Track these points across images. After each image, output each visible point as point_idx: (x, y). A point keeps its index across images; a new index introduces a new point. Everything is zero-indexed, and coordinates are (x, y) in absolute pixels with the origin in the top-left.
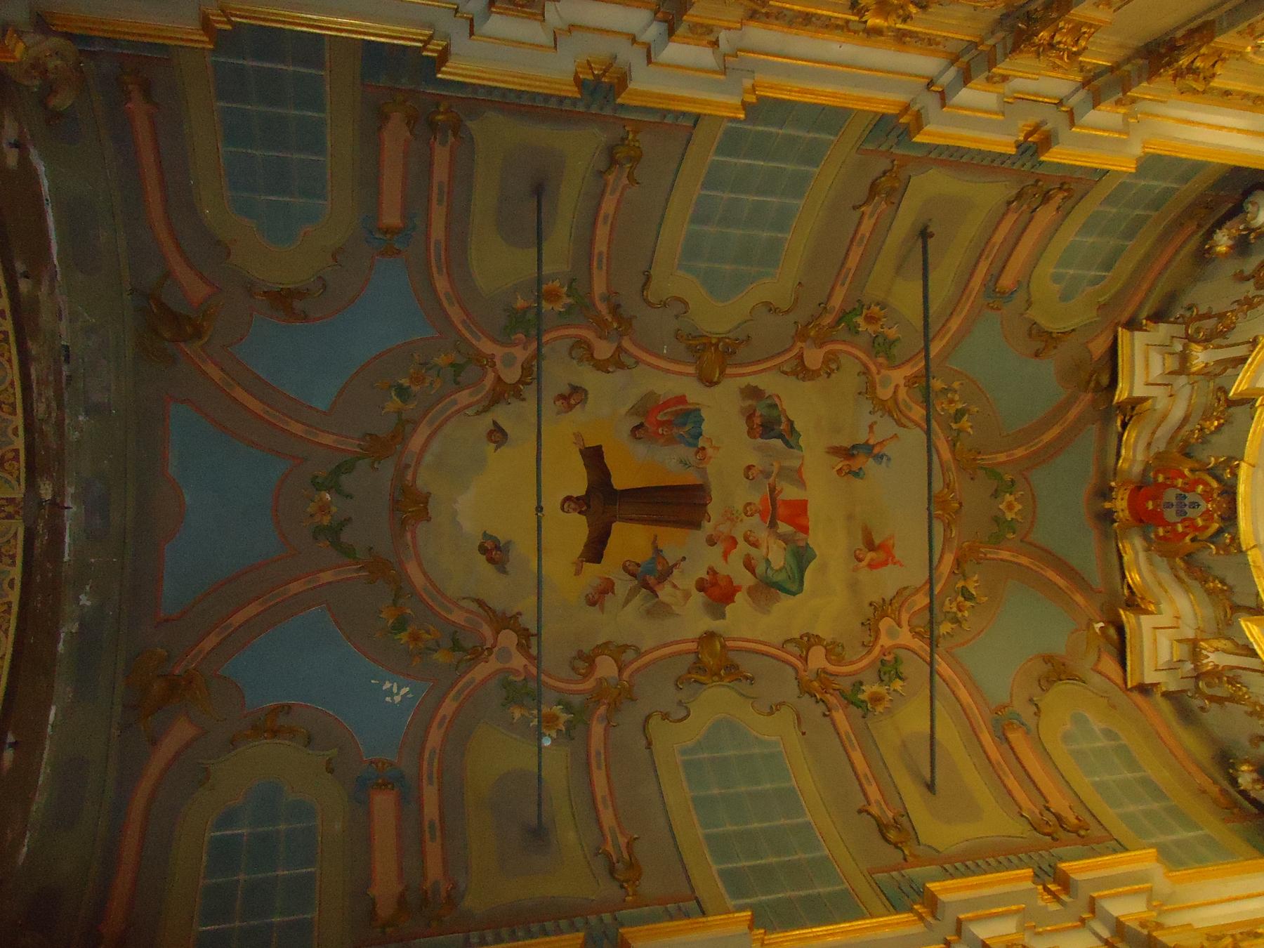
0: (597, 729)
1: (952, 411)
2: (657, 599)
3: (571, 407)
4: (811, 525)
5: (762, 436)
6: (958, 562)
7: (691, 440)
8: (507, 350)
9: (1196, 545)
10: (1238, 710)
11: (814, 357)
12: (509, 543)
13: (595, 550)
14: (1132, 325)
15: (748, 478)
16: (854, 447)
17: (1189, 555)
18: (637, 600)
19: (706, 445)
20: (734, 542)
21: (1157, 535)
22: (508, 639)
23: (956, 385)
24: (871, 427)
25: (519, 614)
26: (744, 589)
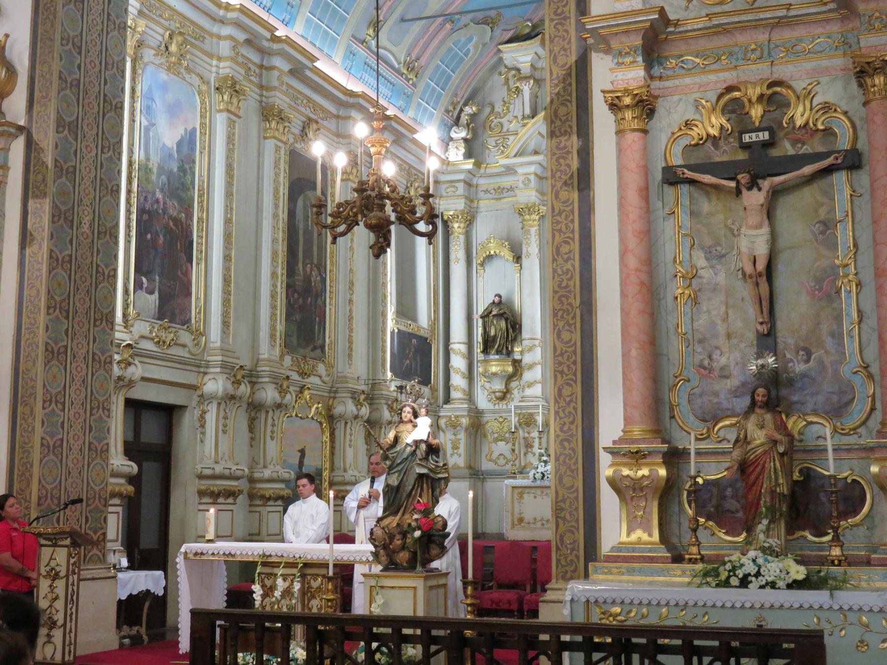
10: (503, 93)
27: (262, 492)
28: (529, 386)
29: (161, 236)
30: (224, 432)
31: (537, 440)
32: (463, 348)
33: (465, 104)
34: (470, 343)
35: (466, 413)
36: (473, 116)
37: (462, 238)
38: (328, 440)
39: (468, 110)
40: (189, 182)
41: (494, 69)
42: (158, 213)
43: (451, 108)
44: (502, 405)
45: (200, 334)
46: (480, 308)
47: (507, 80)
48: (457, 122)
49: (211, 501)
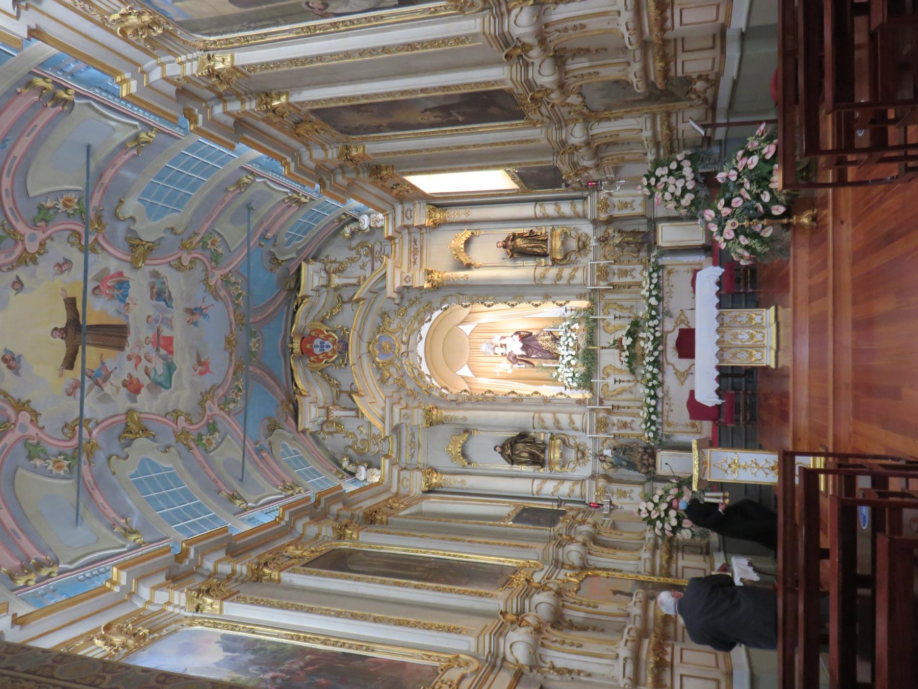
0: (85, 468)
1: (236, 294)
2: (102, 393)
3: (62, 272)
4: (174, 350)
5: (157, 299)
6: (234, 374)
7: (122, 298)
8: (33, 231)
9: (327, 365)
11: (186, 260)
12: (20, 356)
13: (69, 363)
14: (306, 260)
15: (147, 322)
16: (195, 309)
17: (323, 369)
18: (93, 392)
19: (130, 302)
20: (139, 359)
21: (310, 360)
22: (25, 417)
23: (240, 281)
24: (203, 299)
25: (29, 402)
26: (145, 386)
27: (659, 621)
28: (573, 423)
29: (318, 680)
30: (580, 646)
31: (621, 418)
32: (537, 482)
33: (340, 466)
34: (534, 478)
35: (594, 483)
36: (351, 462)
37: (444, 477)
38: (605, 572)
39: (345, 464)
40: (275, 647)
41: (318, 442)
42: (289, 680)
43: (340, 476)
44: (589, 453)
45: (455, 660)
46: (505, 466)
47: (330, 433)
48: (352, 474)
49: (668, 671)
